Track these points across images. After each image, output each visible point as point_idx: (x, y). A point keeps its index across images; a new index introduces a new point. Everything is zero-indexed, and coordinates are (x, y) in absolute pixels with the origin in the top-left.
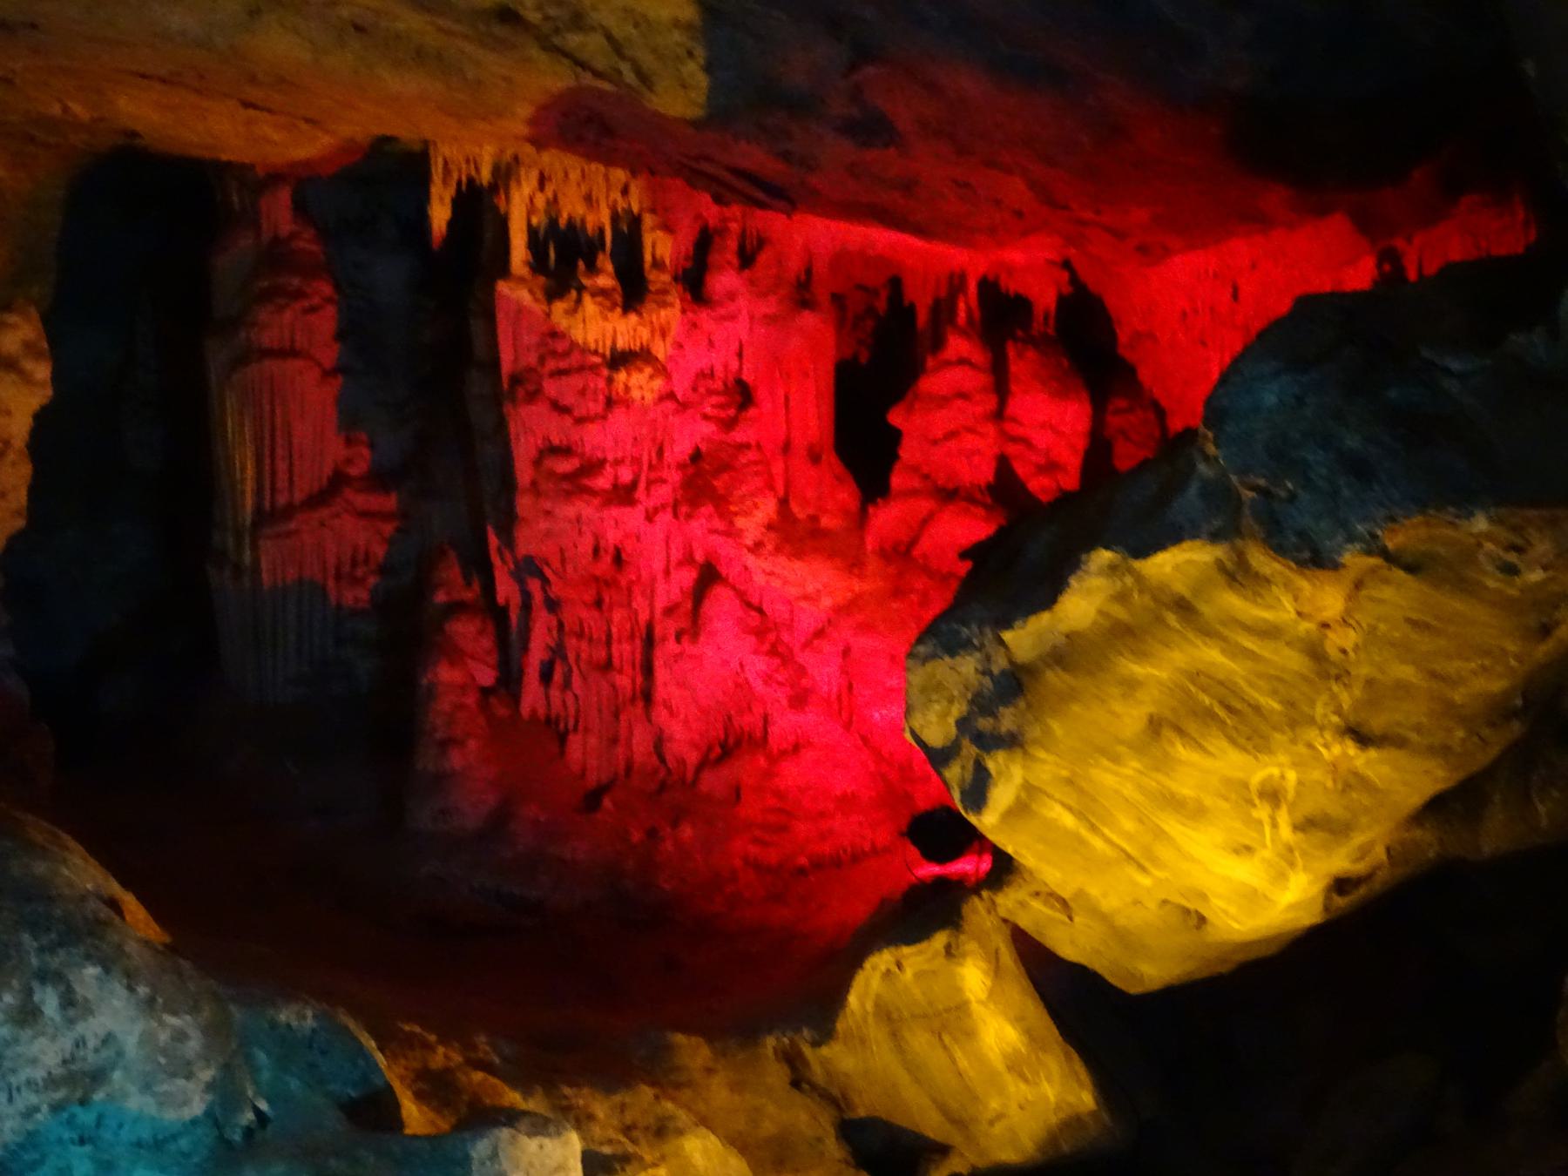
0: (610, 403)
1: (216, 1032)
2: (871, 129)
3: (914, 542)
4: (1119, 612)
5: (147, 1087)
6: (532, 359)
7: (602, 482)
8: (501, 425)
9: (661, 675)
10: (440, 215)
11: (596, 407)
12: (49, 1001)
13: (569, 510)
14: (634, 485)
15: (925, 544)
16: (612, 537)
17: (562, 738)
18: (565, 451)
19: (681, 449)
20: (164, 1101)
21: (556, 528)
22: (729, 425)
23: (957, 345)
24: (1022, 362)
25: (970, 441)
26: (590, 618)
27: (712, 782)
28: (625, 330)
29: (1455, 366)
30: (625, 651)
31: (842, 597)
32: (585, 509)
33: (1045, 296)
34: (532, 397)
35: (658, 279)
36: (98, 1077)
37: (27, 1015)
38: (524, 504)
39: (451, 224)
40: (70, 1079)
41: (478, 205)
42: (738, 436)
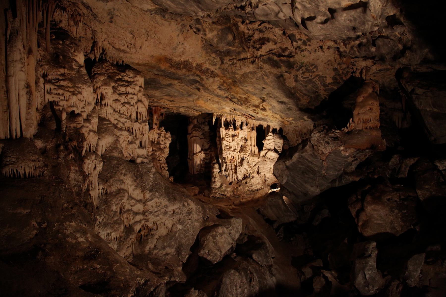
0: (233, 141)
1: (203, 207)
2: (264, 110)
4: (299, 160)
5: (196, 214)
6: (224, 136)
7: (232, 149)
8: (221, 143)
10: (214, 120)
11: (231, 141)
12: (186, 204)
13: (228, 152)
14: (235, 150)
16: (233, 155)
17: (227, 177)
18: (228, 146)
19: (240, 146)
20: (198, 215)
21: (227, 154)
22: (245, 143)
23: (270, 134)
24: (276, 136)
25: (271, 144)
26: (230, 164)
27: (244, 182)
28: (235, 133)
29: (337, 132)
30: (234, 168)
32: (230, 152)
33: (278, 129)
34: (224, 140)
35: (238, 127)
36: (191, 212)
37: (184, 205)
38: (223, 152)
39: (215, 122)
40: (188, 213)
41: (218, 120)
42: (246, 144)
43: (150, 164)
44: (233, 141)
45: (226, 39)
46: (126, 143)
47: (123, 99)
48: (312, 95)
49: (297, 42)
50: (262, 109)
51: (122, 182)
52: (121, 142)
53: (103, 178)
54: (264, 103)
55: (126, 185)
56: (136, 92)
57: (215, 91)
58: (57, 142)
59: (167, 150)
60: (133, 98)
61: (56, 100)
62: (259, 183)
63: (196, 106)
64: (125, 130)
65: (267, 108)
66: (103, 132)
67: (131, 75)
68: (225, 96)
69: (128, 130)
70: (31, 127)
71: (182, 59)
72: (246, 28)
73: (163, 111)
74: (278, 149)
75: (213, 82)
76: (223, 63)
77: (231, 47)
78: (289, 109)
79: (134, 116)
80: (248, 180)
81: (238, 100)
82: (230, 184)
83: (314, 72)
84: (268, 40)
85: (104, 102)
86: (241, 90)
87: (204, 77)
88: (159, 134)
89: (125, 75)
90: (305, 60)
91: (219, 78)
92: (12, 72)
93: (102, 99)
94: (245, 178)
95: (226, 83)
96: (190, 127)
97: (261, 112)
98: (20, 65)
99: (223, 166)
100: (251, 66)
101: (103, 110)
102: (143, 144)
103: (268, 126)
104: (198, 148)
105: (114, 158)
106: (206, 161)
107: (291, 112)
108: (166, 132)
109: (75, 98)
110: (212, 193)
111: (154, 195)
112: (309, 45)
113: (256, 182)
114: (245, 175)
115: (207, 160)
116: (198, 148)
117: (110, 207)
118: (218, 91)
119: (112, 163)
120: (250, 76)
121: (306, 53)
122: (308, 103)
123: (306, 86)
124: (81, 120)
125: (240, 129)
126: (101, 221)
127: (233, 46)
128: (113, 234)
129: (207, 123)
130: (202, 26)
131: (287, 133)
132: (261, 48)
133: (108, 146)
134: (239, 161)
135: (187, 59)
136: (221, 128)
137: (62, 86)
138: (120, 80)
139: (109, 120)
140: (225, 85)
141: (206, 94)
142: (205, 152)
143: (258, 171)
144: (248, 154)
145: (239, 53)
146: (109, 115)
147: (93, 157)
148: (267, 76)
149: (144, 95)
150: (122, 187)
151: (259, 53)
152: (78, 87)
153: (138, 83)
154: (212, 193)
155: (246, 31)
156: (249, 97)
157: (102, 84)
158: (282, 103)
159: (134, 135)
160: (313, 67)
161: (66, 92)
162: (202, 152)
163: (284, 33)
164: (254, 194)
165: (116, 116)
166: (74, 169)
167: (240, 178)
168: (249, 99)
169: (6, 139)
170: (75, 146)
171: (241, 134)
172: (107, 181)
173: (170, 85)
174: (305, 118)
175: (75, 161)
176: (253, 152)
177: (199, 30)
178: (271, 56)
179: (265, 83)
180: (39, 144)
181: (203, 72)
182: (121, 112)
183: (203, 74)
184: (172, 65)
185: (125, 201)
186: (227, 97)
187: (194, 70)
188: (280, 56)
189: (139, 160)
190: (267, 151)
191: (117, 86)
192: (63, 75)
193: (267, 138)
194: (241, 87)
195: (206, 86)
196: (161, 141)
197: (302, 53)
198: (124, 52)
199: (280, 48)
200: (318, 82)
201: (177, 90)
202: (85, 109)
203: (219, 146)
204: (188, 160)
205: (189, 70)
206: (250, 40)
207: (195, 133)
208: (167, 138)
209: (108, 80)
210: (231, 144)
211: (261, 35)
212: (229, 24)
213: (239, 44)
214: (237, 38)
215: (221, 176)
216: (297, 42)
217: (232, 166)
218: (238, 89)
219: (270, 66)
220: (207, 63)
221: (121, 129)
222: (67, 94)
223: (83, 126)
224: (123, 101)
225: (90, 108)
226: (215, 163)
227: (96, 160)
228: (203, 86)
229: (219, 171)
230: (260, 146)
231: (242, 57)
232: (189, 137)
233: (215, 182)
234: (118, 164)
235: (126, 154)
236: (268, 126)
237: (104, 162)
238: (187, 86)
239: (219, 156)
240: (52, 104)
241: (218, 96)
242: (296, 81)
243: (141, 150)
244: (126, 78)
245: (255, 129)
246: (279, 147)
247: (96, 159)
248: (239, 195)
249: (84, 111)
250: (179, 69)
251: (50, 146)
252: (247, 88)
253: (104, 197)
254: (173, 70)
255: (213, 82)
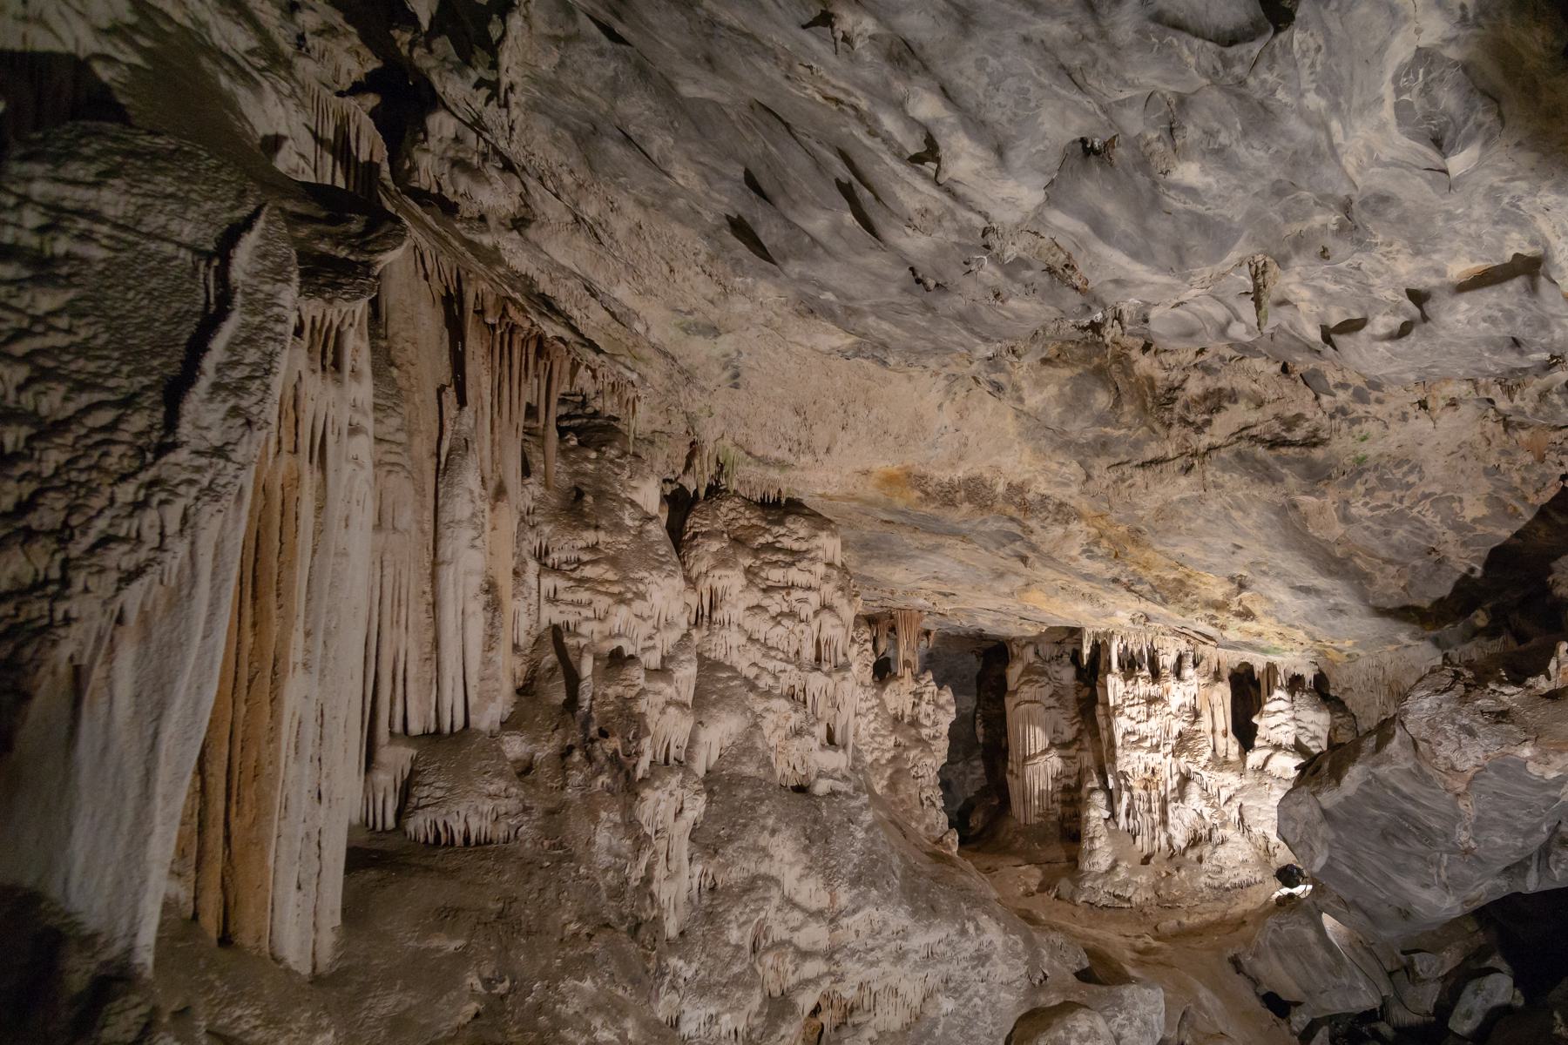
0: (1149, 716)
2: (1246, 615)
3: (1265, 765)
6: (1119, 701)
7: (1147, 744)
8: (1110, 724)
9: (1170, 814)
10: (1086, 651)
13: (1135, 754)
15: (1269, 767)
16: (1152, 765)
18: (1133, 733)
19: (1175, 733)
21: (1132, 762)
22: (1193, 723)
23: (1278, 693)
26: (1143, 793)
27: (1192, 855)
28: (1154, 690)
30: (1156, 805)
31: (1238, 786)
32: (1142, 753)
33: (1309, 674)
34: (1121, 714)
35: (1165, 672)
38: (1119, 752)
41: (1099, 649)
43: (858, 797)
44: (1149, 716)
45: (1087, 406)
46: (782, 733)
47: (775, 603)
48: (1419, 562)
49: (1334, 395)
50: (1238, 614)
51: (764, 853)
52: (766, 732)
53: (705, 842)
54: (1245, 594)
55: (777, 865)
56: (814, 582)
57: (1073, 564)
58: (564, 739)
59: (943, 745)
60: (805, 601)
61: (572, 619)
62: (1244, 862)
63: (1025, 609)
64: (781, 696)
65: (1257, 609)
66: (714, 705)
67: (803, 533)
68: (1108, 576)
69: (791, 696)
70: (493, 699)
71: (960, 474)
72: (1156, 364)
73: (928, 623)
74: (1310, 744)
75: (1066, 536)
76: (1089, 477)
77: (1108, 429)
78: (1338, 611)
79: (809, 653)
80: (1207, 850)
81: (1154, 589)
82: (1146, 860)
83: (1409, 486)
84: (1233, 397)
85: (717, 615)
86: (1159, 557)
87: (1033, 524)
88: (918, 695)
89: (782, 531)
90: (1370, 450)
91: (1083, 524)
92: (449, 554)
93: (713, 607)
94: (1195, 841)
95: (1109, 539)
96: (1014, 673)
97: (1237, 622)
98: (472, 533)
99: (1120, 800)
100: (1183, 481)
101: (715, 639)
102: (838, 738)
103: (1271, 668)
104: (1038, 738)
105: (742, 780)
106: (1065, 781)
107: (1345, 618)
108: (940, 688)
109: (623, 611)
110: (1084, 890)
111: (863, 895)
112: (1379, 401)
113: (1235, 857)
114: (1195, 831)
115: (1068, 777)
116: (1038, 738)
117: (720, 931)
118: (1084, 561)
119: (733, 796)
120: (1186, 511)
121: (1370, 427)
122: (1404, 588)
123: (1387, 533)
124: (636, 674)
125: (1172, 678)
126: (689, 975)
127: (1117, 424)
128: (726, 1018)
129: (1067, 659)
130: (1009, 374)
131: (1346, 690)
132: (1208, 422)
133: (727, 743)
134: (1173, 783)
135: (976, 472)
136: (1109, 677)
137: (588, 580)
138: (770, 547)
139: (732, 668)
140: (1105, 543)
141: (1049, 573)
142: (1064, 753)
143: (1242, 819)
144: (1203, 760)
145: (1137, 445)
146: (735, 652)
147: (674, 780)
148: (1240, 508)
149: (841, 589)
150: (764, 868)
151: (1204, 441)
152: (634, 580)
153: (821, 554)
154: (1084, 890)
155: (1159, 374)
156: (1189, 576)
157: (712, 562)
158: (1307, 590)
159: (809, 710)
160: (1405, 468)
161: (600, 597)
162: (1053, 751)
163: (1285, 369)
164: (1230, 900)
165: (755, 653)
166: (608, 820)
167: (1180, 840)
168: (1191, 582)
169: (425, 734)
170: (616, 752)
171: (1179, 694)
172: (716, 852)
173: (935, 549)
174: (1403, 637)
175: (613, 795)
176: (1221, 754)
177: (998, 388)
178: (1244, 445)
179: (1237, 531)
180: (515, 747)
181: (1025, 507)
182: (770, 643)
183: (1029, 515)
184: (927, 494)
185: (771, 914)
186: (1115, 580)
187: (998, 506)
188: (1275, 443)
189: (822, 787)
190: (1268, 752)
191: (760, 567)
192: (593, 548)
193: (1266, 708)
194: (1158, 547)
195: (1045, 548)
196: (921, 716)
197: (1356, 428)
198: (782, 465)
199: (1277, 417)
200: (1431, 518)
201: (961, 562)
202: (657, 641)
203: (1105, 735)
204: (1008, 777)
205: (983, 507)
206: (1173, 400)
207: (1027, 692)
208: (942, 707)
209: (730, 552)
210: (1143, 728)
211: (1210, 382)
212: (1096, 361)
213: (1135, 417)
214: (1125, 398)
215: (1113, 834)
216: (1334, 395)
217: (1149, 801)
218: (1148, 554)
219: (1247, 479)
220: (1040, 479)
221: (768, 694)
222: (602, 603)
223: (643, 692)
224: (775, 609)
225: (673, 636)
226: (1093, 790)
227: (684, 787)
228: (1034, 548)
229: (1106, 814)
230: (1245, 733)
231: (1149, 456)
232: (1010, 702)
233: (1091, 852)
234: (755, 799)
235: (781, 768)
236: (1271, 668)
237: (710, 792)
238: (986, 549)
239: (1107, 766)
240: (557, 632)
241: (1088, 577)
242: (1346, 519)
243: (830, 753)
244: (787, 542)
245: (1225, 676)
246: (1315, 738)
247: (683, 785)
248: (1174, 901)
249: (654, 647)
250: (951, 503)
251: (545, 750)
252: (1179, 550)
253: (706, 902)
254: (930, 509)
255: (1066, 536)
